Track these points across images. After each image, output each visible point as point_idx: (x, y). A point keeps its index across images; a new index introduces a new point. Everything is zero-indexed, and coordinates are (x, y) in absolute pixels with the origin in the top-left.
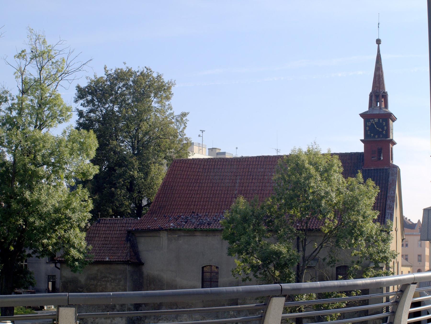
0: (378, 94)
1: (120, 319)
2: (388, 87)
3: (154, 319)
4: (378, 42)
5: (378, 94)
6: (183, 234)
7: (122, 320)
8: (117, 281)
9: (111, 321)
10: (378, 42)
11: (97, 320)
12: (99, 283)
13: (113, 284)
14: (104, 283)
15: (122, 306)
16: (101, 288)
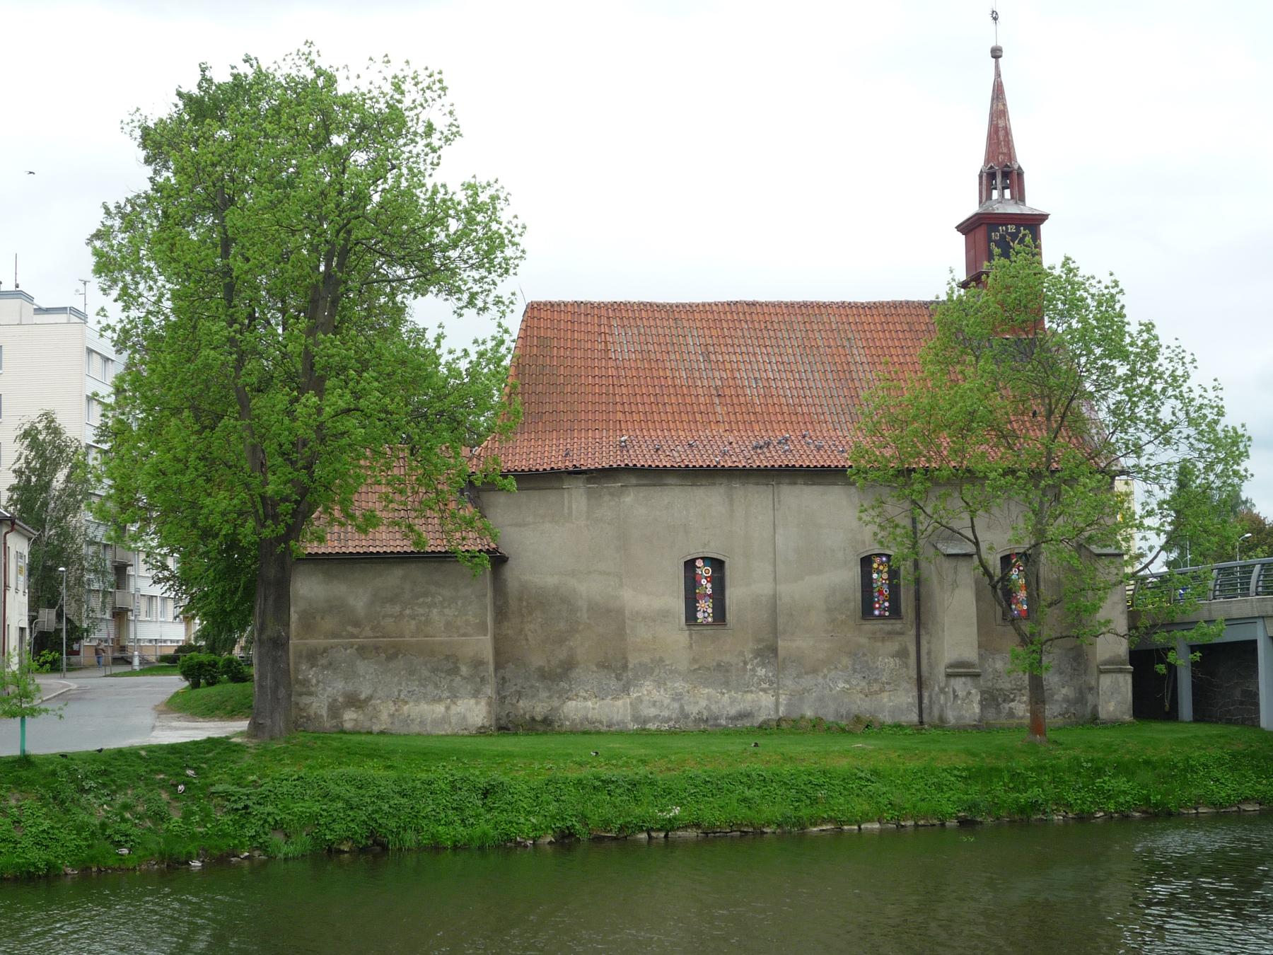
0: (1002, 172)
1: (472, 701)
2: (1024, 157)
3: (550, 697)
4: (996, 53)
5: (1002, 172)
6: (634, 481)
7: (477, 703)
8: (460, 603)
9: (448, 708)
10: (996, 53)
11: (406, 708)
12: (408, 612)
13: (447, 611)
14: (421, 611)
15: (476, 667)
16: (413, 622)
